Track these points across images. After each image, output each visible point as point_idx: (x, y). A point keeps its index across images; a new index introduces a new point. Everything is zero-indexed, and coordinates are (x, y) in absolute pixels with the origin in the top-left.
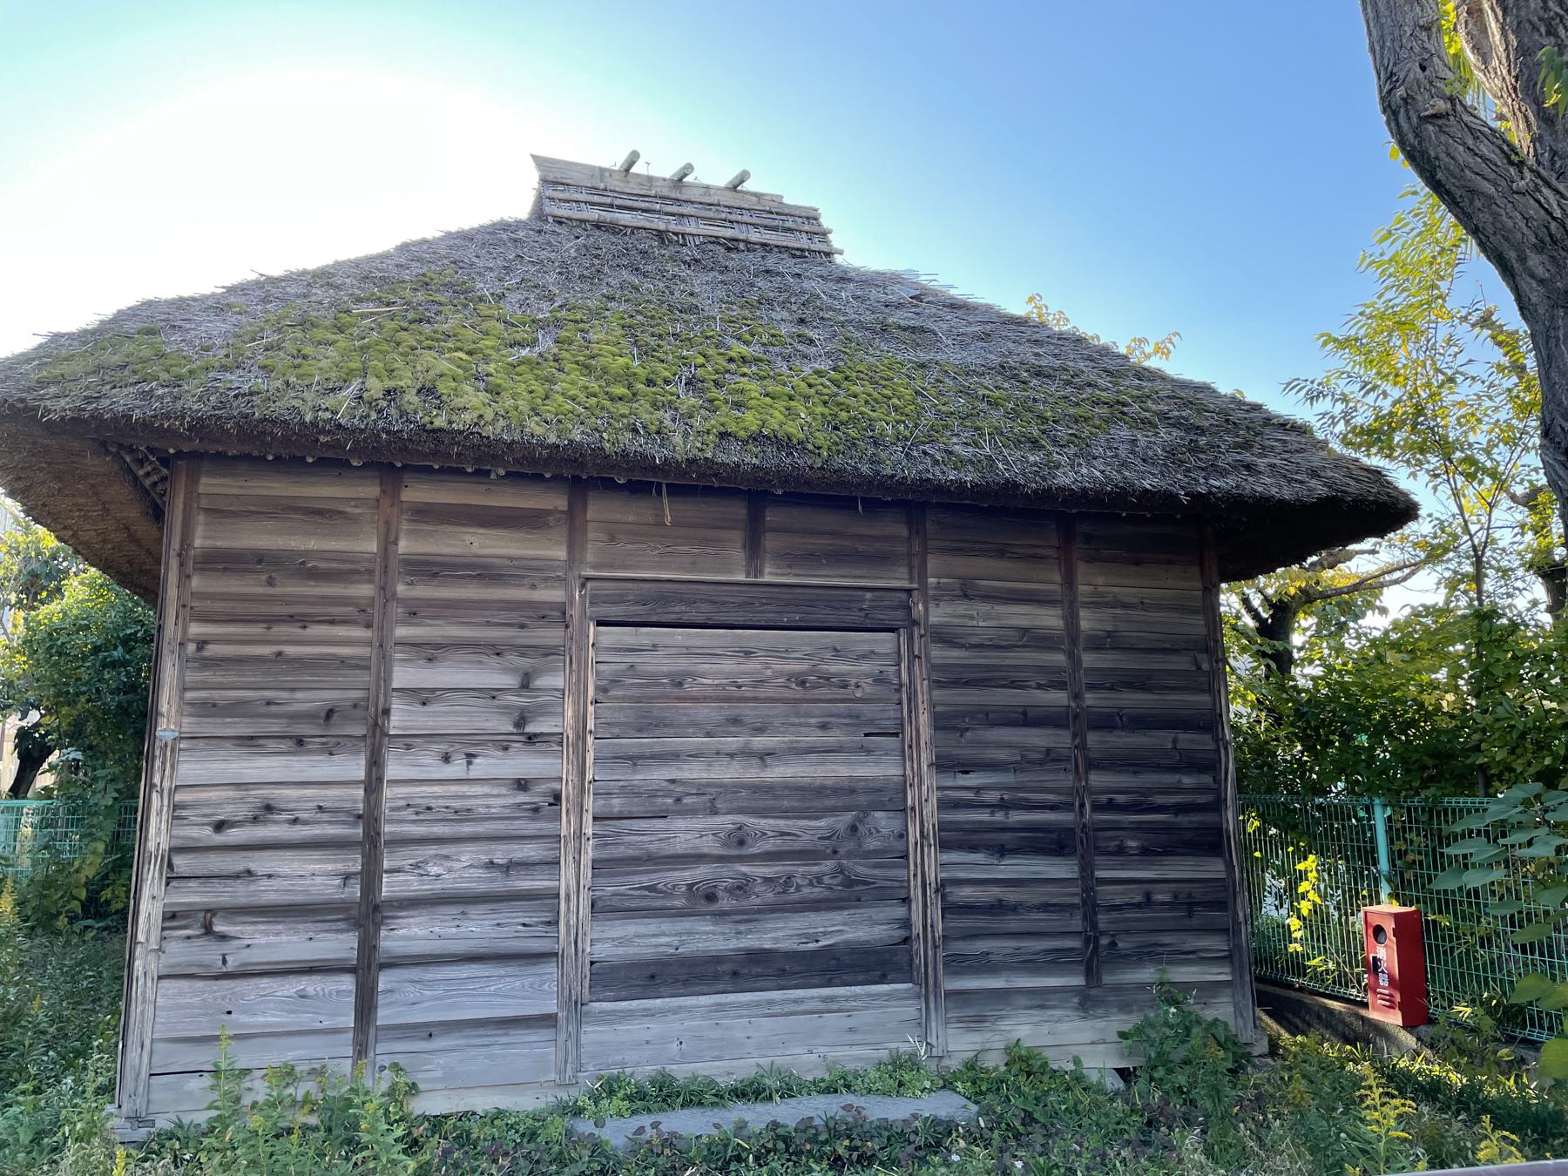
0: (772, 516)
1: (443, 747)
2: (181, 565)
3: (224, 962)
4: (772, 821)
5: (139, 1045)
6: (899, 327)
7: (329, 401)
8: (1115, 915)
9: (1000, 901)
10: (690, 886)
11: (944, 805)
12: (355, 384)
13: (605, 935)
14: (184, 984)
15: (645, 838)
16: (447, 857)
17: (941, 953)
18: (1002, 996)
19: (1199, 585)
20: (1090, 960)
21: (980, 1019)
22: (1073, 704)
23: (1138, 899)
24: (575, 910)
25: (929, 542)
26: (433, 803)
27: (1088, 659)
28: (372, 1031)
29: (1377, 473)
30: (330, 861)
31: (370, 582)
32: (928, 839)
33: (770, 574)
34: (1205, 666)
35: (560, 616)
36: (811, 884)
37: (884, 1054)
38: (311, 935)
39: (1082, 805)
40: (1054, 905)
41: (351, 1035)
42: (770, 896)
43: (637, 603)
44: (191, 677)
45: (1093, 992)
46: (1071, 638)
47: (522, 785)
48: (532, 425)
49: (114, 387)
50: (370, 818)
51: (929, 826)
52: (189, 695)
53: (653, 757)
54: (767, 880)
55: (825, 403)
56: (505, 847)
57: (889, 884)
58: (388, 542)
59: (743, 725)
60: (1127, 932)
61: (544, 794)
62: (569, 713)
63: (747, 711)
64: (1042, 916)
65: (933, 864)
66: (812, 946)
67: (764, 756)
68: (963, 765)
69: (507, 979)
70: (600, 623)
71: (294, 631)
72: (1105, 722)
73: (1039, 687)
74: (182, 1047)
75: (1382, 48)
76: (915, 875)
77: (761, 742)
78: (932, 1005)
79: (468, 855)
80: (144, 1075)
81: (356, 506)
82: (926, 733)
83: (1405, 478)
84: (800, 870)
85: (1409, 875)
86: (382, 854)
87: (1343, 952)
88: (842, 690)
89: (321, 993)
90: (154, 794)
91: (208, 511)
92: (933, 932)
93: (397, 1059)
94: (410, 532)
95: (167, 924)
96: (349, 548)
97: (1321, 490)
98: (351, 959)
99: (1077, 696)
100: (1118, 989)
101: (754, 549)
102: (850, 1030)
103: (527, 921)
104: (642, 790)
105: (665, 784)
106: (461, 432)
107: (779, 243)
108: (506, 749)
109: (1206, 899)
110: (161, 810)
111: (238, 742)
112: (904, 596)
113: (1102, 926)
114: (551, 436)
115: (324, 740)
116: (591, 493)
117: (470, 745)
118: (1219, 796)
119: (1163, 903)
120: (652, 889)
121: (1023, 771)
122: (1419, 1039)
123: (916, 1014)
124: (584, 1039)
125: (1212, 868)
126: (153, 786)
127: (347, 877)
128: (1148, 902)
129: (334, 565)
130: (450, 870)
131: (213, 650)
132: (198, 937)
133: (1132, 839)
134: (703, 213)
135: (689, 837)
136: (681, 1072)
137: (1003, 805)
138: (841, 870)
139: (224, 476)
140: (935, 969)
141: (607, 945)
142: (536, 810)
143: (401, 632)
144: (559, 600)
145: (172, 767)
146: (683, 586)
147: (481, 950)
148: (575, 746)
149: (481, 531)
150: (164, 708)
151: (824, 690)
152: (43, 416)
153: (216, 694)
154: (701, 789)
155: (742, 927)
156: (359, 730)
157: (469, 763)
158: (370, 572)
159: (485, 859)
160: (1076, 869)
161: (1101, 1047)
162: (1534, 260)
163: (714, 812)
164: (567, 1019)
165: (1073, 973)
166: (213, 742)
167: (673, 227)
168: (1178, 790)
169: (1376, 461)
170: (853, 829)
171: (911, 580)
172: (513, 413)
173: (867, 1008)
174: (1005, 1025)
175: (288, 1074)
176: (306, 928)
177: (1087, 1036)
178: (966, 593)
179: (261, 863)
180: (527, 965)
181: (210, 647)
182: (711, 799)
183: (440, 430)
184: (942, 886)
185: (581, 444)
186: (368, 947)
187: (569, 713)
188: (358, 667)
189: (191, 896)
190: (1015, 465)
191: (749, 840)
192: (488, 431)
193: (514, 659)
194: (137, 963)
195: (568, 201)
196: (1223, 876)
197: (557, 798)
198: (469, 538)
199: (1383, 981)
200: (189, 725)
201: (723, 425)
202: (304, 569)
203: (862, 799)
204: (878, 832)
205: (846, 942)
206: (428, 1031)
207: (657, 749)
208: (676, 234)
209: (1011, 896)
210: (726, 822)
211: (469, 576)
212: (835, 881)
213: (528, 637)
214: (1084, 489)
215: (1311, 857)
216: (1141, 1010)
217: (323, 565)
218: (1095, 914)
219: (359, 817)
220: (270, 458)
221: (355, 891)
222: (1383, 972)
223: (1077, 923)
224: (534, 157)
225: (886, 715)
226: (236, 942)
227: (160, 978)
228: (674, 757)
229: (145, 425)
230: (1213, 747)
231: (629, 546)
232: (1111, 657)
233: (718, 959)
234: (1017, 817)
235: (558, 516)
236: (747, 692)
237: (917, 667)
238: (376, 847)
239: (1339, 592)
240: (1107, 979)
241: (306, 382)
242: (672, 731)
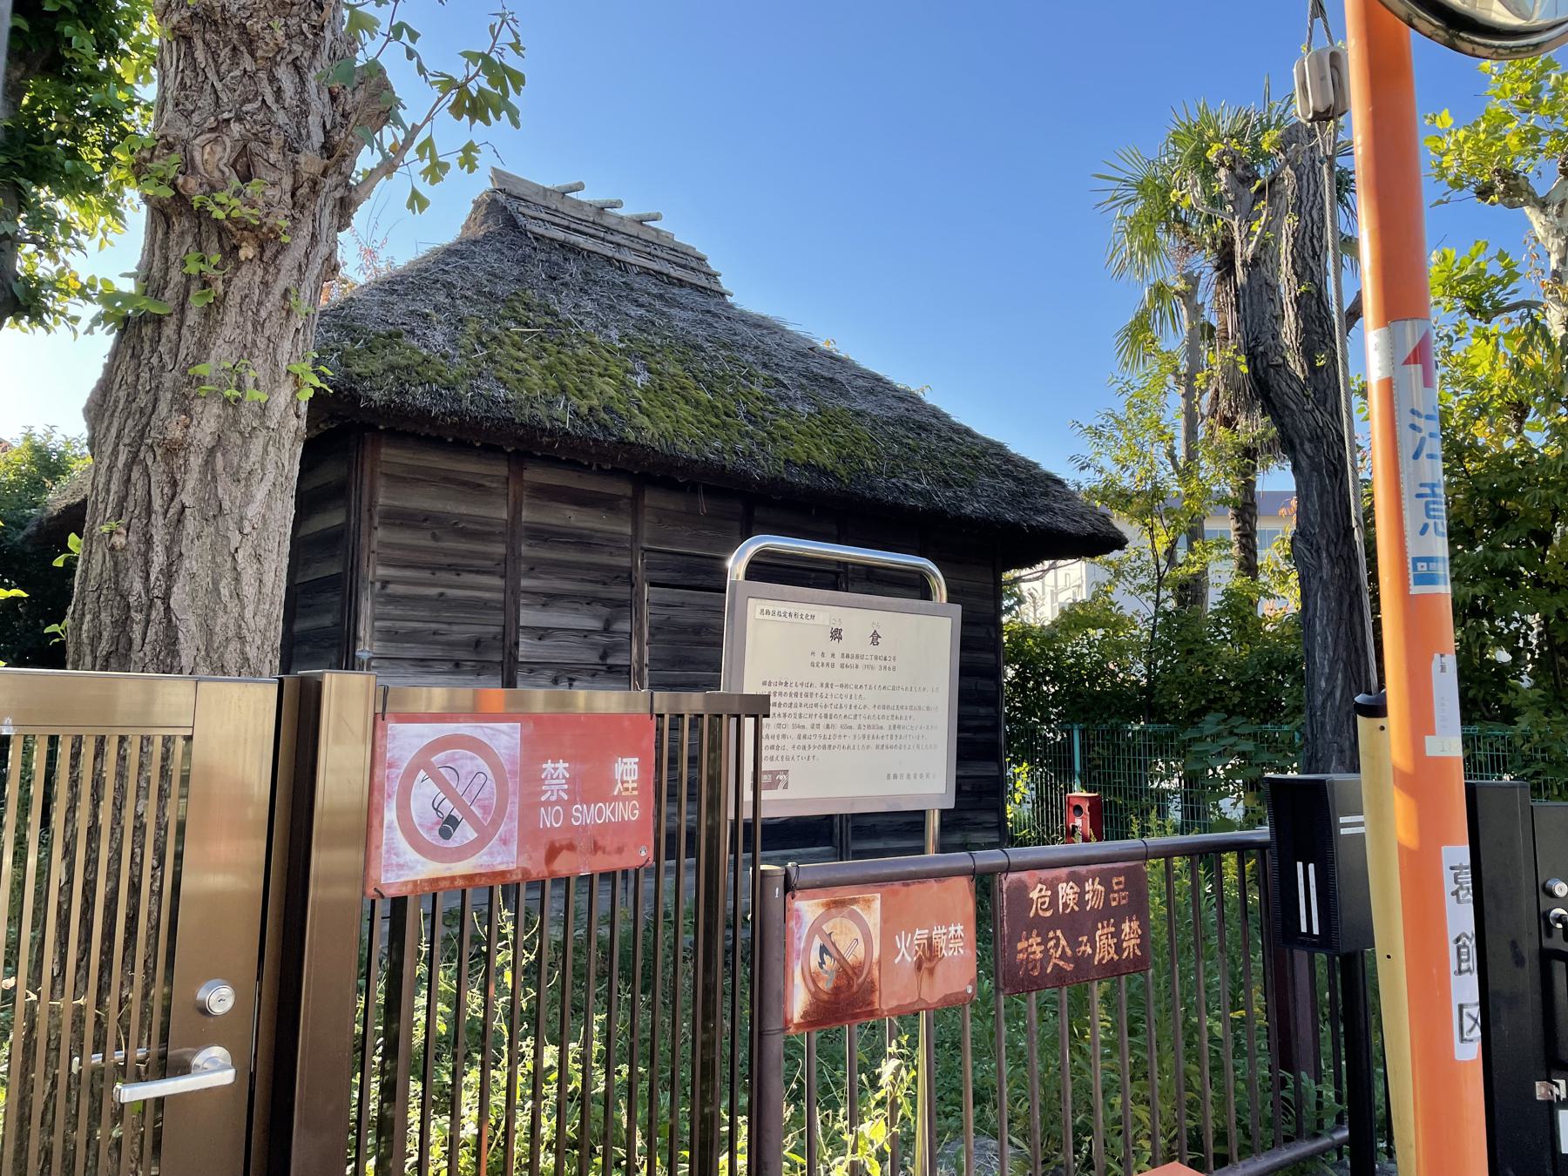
0: (758, 513)
17: (850, 825)
19: (992, 580)
35: (627, 577)
43: (674, 571)
44: (379, 609)
52: (377, 624)
62: (635, 650)
70: (652, 584)
75: (1252, 321)
83: (1122, 523)
85: (1095, 773)
97: (1089, 529)
106: (643, 446)
108: (594, 675)
112: (833, 577)
129: (478, 527)
143: (525, 583)
153: (398, 624)
156: (498, 658)
162: (1307, 446)
187: (635, 650)
188: (496, 608)
190: (942, 497)
198: (568, 513)
208: (619, 261)
215: (1025, 764)
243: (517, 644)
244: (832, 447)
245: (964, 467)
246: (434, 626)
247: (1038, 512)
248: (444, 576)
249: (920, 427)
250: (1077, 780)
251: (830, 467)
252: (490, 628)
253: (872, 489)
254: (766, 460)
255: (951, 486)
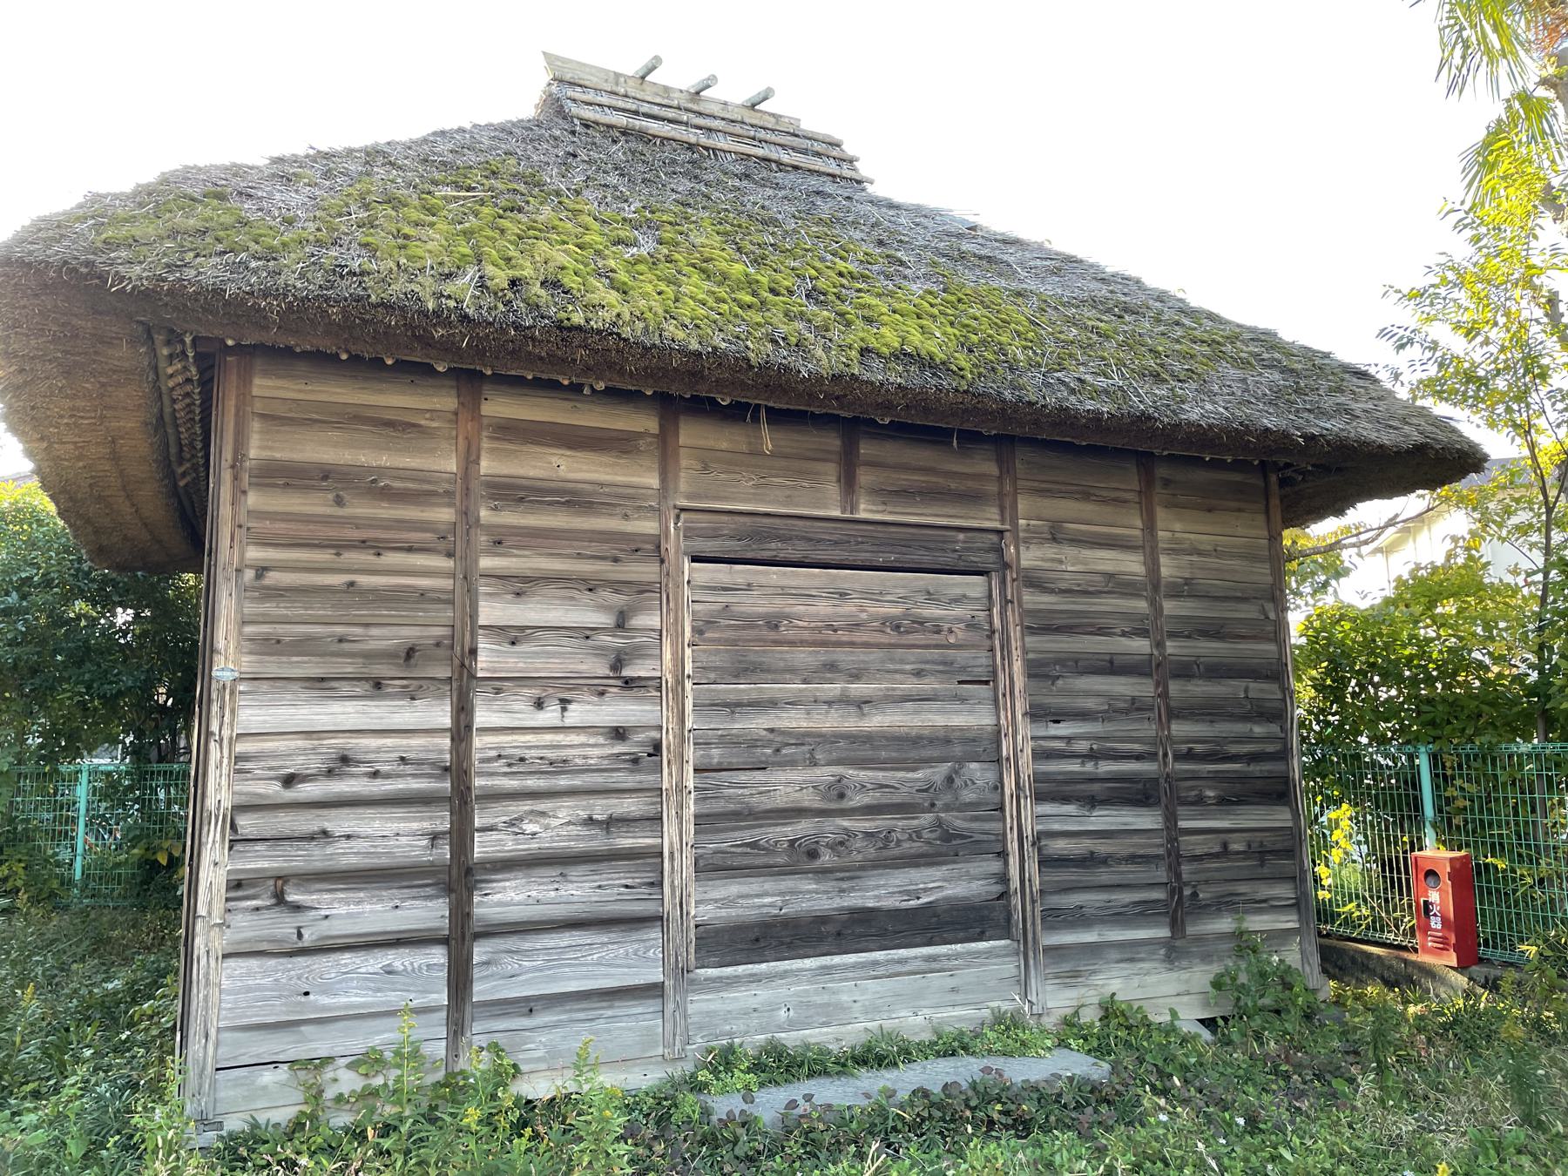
0: (866, 449)
1: (536, 692)
2: (236, 478)
3: (300, 936)
4: (870, 773)
5: (203, 1034)
6: (975, 255)
7: (449, 288)
8: (1195, 866)
9: (1092, 853)
10: (792, 842)
11: (1040, 755)
12: (471, 271)
13: (707, 896)
14: (253, 963)
15: (746, 792)
16: (543, 814)
17: (1038, 909)
18: (1094, 950)
19: (1266, 533)
20: (1175, 911)
21: (1076, 974)
22: (1155, 652)
23: (1217, 849)
24: (680, 870)
25: (1019, 482)
26: (528, 754)
27: (1169, 607)
28: (468, 1009)
29: (1442, 424)
30: (415, 819)
31: (449, 505)
32: (1024, 792)
33: (865, 510)
34: (1272, 616)
35: (655, 549)
36: (910, 839)
37: (986, 1013)
38: (398, 902)
39: (1166, 755)
40: (1141, 856)
41: (444, 1014)
42: (871, 852)
44: (250, 608)
45: (1178, 943)
46: (1153, 586)
47: (619, 734)
48: (672, 328)
49: (197, 255)
50: (458, 770)
51: (1024, 777)
52: (248, 629)
53: (750, 704)
54: (868, 835)
55: (952, 324)
56: (600, 802)
57: (985, 837)
58: (470, 460)
59: (840, 671)
60: (1206, 882)
61: (642, 744)
62: (667, 655)
63: (843, 656)
64: (1131, 868)
65: (1030, 816)
66: (913, 903)
67: (861, 704)
68: (1054, 714)
69: (610, 947)
70: (695, 559)
71: (365, 558)
72: (1184, 671)
73: (1124, 634)
74: (248, 1034)
76: (1011, 828)
77: (858, 689)
78: (1031, 962)
79: (566, 810)
80: (209, 1069)
81: (432, 419)
82: (1020, 682)
84: (900, 824)
86: (473, 811)
87: (1379, 898)
88: (936, 636)
89: (409, 968)
90: (212, 745)
91: (263, 417)
92: (1031, 886)
93: (497, 1037)
94: (492, 450)
95: (232, 894)
96: (426, 467)
97: (1417, 438)
98: (443, 929)
99: (1159, 645)
100: (1200, 939)
101: (848, 483)
102: (953, 990)
103: (629, 882)
104: (741, 740)
105: (765, 733)
106: (599, 332)
107: (812, 167)
108: (602, 694)
109: (1278, 846)
110: (221, 762)
111: (307, 684)
112: (994, 538)
113: (1185, 877)
114: (693, 341)
115: (405, 682)
116: (682, 418)
117: (563, 691)
118: (1285, 745)
119: (1238, 853)
120: (753, 845)
121: (1110, 720)
122: (1470, 979)
123: (1014, 972)
124: (691, 1009)
125: (1279, 817)
126: (209, 734)
127: (435, 837)
128: (1225, 852)
129: (411, 485)
130: (547, 828)
131: (273, 578)
132: (268, 908)
133: (1210, 788)
134: (730, 128)
135: (789, 790)
136: (791, 1039)
137: (1092, 756)
138: (939, 824)
139: (279, 377)
140: (1034, 923)
141: (709, 907)
142: (636, 761)
143: (486, 563)
144: (652, 532)
145: (233, 711)
146: (777, 521)
147: (584, 915)
148: (675, 691)
149: (568, 453)
150: (220, 643)
151: (916, 636)
152: (112, 286)
153: (280, 629)
154: (801, 738)
155: (845, 885)
156: (444, 672)
157: (564, 709)
158: (448, 493)
159: (583, 814)
160: (1160, 819)
161: (1185, 999)
163: (814, 763)
164: (675, 988)
165: (1157, 925)
166: (279, 684)
167: (704, 140)
168: (1251, 739)
169: (1441, 409)
170: (950, 780)
171: (1003, 521)
172: (648, 315)
173: (968, 966)
174: (1098, 979)
175: (369, 1061)
176: (392, 895)
177: (1171, 989)
178: (1055, 534)
179: (339, 822)
180: (631, 930)
181: (271, 574)
182: (809, 747)
183: (579, 328)
184: (1039, 837)
185: (725, 354)
186: (461, 914)
187: (667, 655)
188: (439, 601)
189: (260, 861)
190: (1146, 398)
191: (849, 793)
192: (626, 332)
193: (606, 595)
194: (197, 941)
195: (591, 104)
196: (1290, 824)
197: (657, 748)
198: (555, 460)
199: (1435, 923)
200: (248, 663)
201: (862, 340)
202: (376, 487)
203: (957, 750)
204: (974, 783)
205: (946, 899)
206: (528, 1006)
207: (754, 696)
208: (707, 149)
209: (1102, 847)
210: (825, 774)
211: (558, 502)
212: (933, 835)
213: (619, 572)
214: (1210, 426)
215: (1345, 806)
216: (1220, 959)
217: (397, 484)
218: (1179, 864)
219: (446, 769)
220: (344, 357)
221: (445, 852)
222: (1435, 915)
223: (1161, 874)
224: (544, 53)
225: (978, 662)
226: (313, 913)
227: (225, 956)
228: (773, 704)
229: (238, 302)
230: (1280, 696)
231: (723, 476)
232: (1189, 604)
233: (823, 919)
234: (1106, 767)
235: (649, 440)
236: (843, 636)
237: (1009, 613)
238: (466, 803)
239: (1316, 551)
240: (1191, 930)
241: (418, 265)
242: (773, 676)
243: (473, 652)
244: (949, 330)
245: (1192, 357)
246: (339, 630)
247: (1321, 413)
248: (352, 557)
249: (1126, 310)
250: (1429, 831)
251: (940, 356)
252: (427, 628)
253: (1015, 387)
254: (827, 349)
255: (1165, 381)
